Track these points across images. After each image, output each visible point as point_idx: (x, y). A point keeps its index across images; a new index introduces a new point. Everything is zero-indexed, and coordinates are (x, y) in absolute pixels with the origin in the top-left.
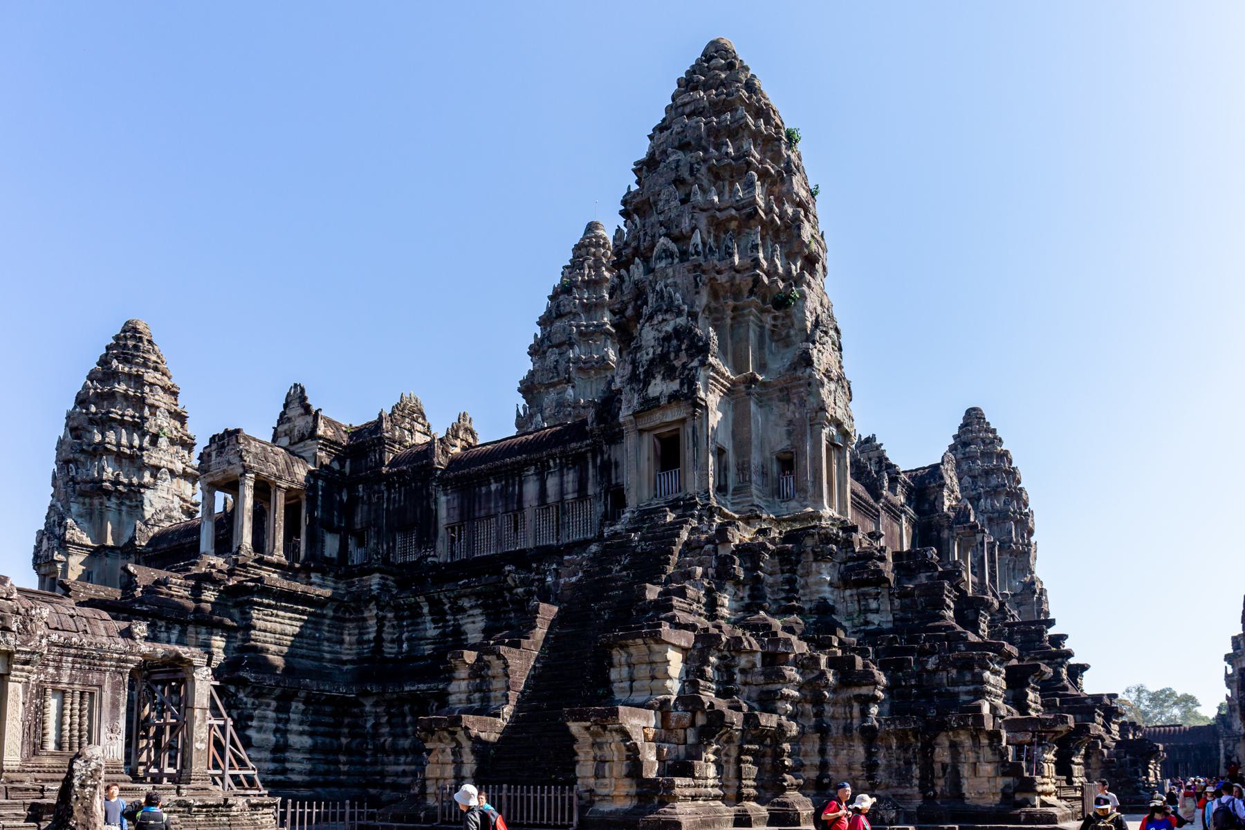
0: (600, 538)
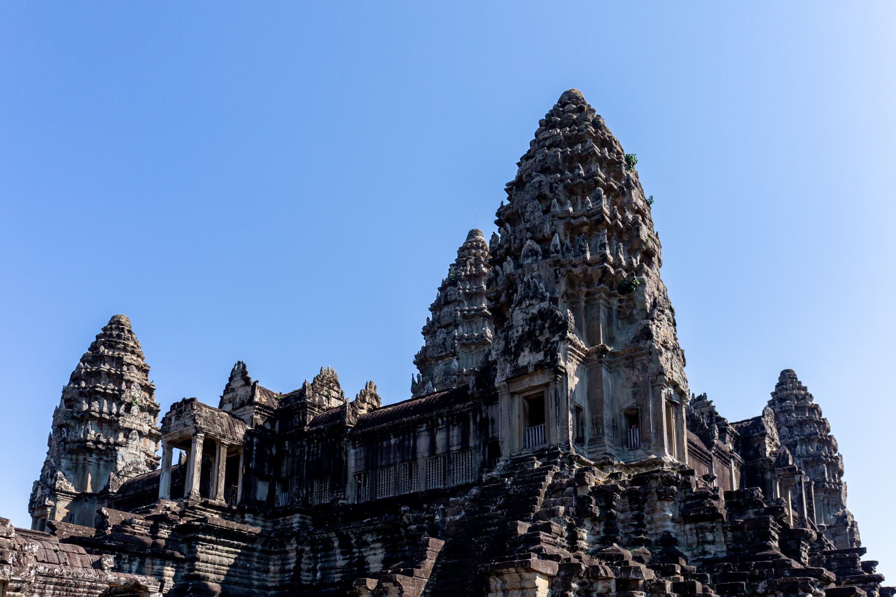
0: (479, 483)
